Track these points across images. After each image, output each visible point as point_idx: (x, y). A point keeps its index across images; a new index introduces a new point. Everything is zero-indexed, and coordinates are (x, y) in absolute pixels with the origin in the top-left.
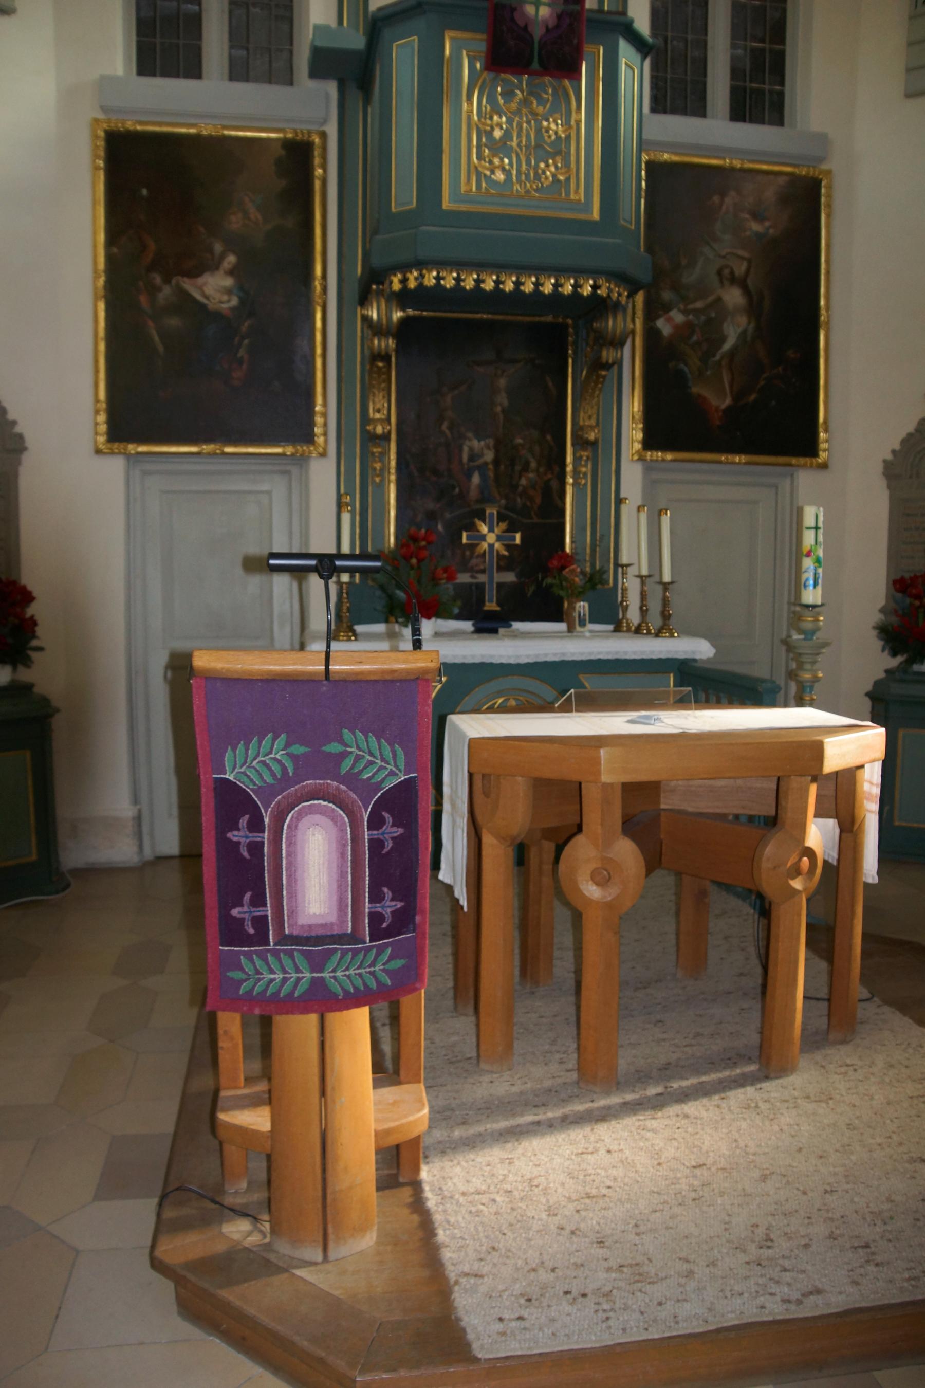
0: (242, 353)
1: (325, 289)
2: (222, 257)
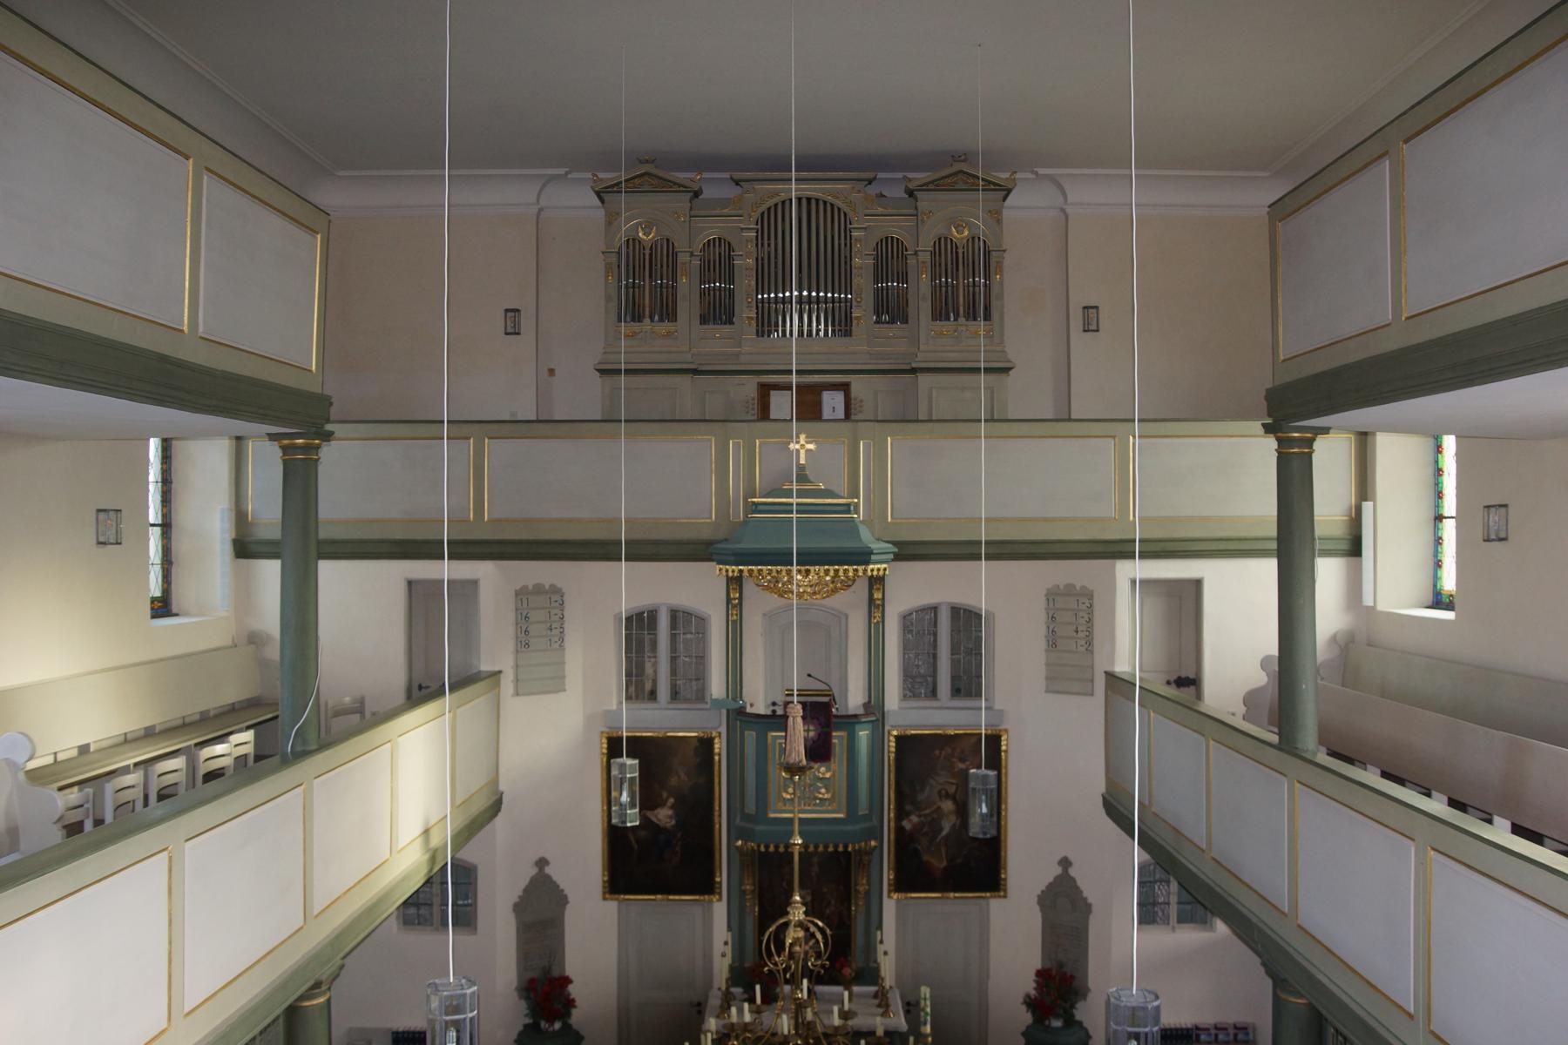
1: (720, 816)
2: (666, 801)
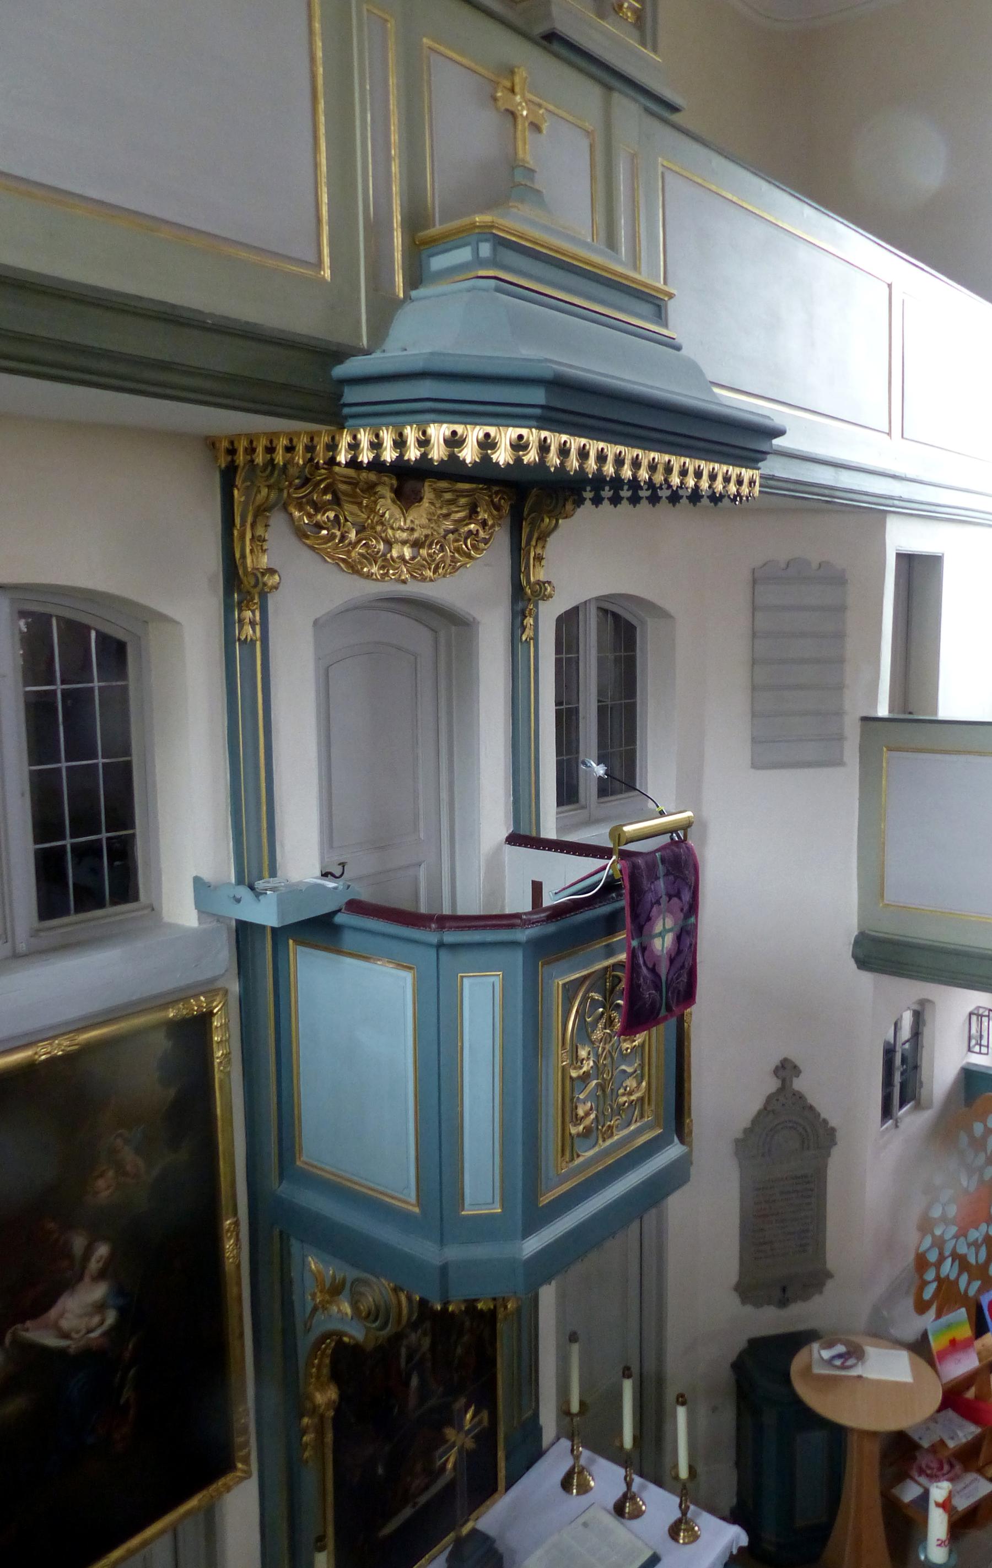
0: (127, 1394)
